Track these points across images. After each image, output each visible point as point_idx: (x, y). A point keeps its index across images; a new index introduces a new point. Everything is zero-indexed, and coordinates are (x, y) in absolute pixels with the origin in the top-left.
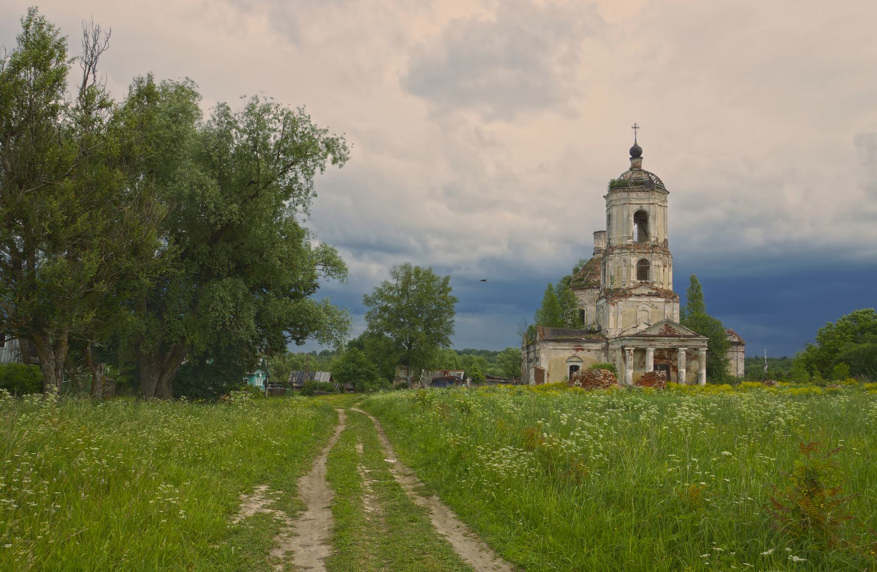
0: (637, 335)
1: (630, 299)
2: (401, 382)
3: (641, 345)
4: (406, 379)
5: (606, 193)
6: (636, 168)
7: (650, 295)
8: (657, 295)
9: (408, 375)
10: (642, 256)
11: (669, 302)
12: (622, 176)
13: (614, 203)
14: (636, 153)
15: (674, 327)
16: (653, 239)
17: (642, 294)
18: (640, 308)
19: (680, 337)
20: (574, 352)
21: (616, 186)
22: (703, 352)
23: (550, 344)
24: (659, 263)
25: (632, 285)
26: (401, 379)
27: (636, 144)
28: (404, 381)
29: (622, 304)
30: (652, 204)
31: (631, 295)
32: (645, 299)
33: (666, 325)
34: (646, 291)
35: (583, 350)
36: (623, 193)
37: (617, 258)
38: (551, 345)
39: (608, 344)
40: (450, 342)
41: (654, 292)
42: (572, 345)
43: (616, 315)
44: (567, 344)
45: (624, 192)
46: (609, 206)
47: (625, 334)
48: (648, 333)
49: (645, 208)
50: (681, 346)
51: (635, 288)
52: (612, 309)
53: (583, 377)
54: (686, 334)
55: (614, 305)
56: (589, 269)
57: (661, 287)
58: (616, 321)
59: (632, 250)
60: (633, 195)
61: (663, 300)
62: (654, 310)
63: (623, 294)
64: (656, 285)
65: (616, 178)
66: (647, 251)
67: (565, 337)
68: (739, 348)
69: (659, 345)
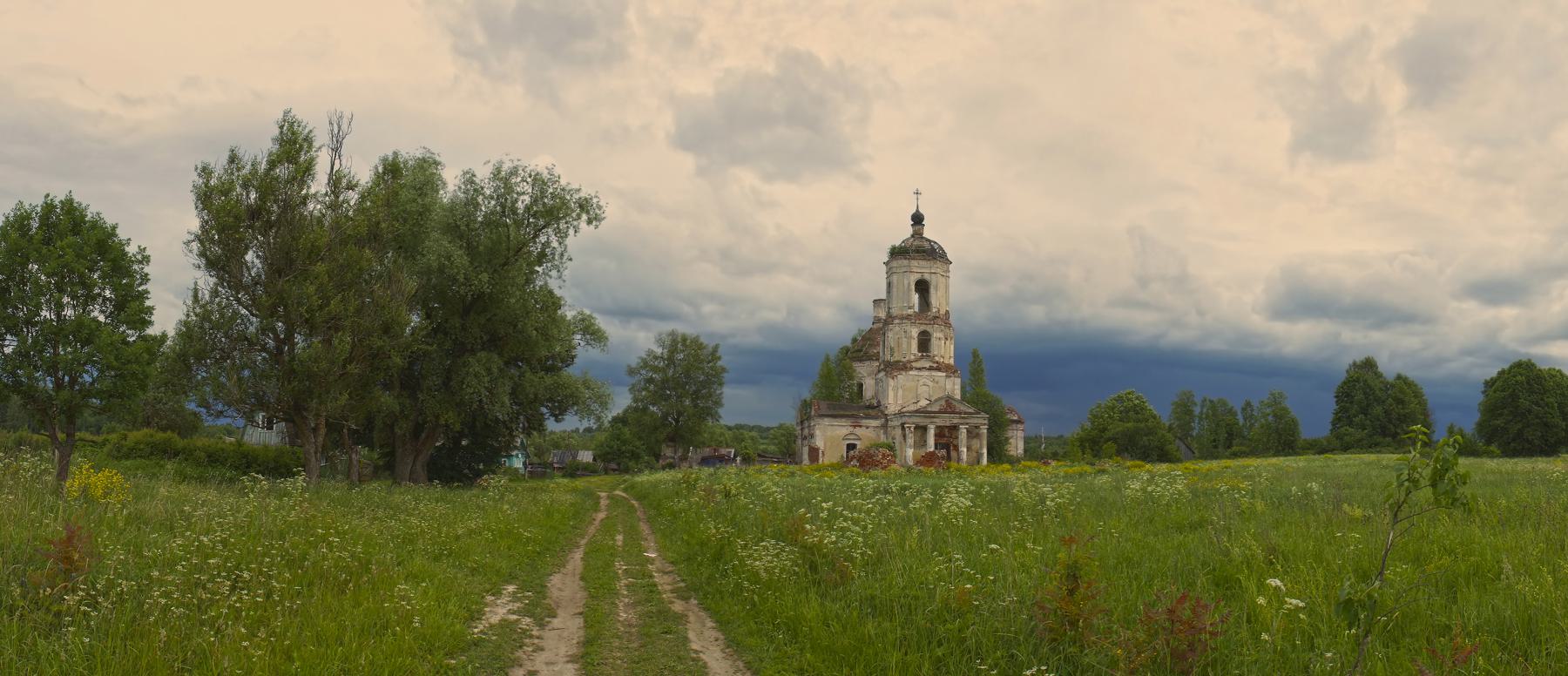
0: (917, 411)
1: (911, 373)
2: (668, 461)
3: (921, 421)
4: (673, 458)
5: (886, 259)
6: (918, 234)
7: (931, 369)
8: (938, 369)
9: (675, 453)
10: (923, 328)
11: (951, 377)
12: (903, 242)
13: (894, 270)
14: (918, 219)
15: (954, 403)
17: (923, 368)
18: (921, 383)
19: (960, 414)
20: (851, 429)
21: (897, 253)
22: (984, 431)
23: (826, 419)
24: (940, 335)
25: (913, 357)
26: (668, 458)
27: (917, 211)
28: (672, 460)
29: (902, 378)
30: (935, 273)
31: (911, 369)
32: (927, 373)
33: (947, 401)
34: (927, 366)
35: (860, 426)
36: (904, 261)
37: (897, 328)
38: (827, 421)
39: (887, 420)
40: (720, 417)
41: (935, 365)
42: (849, 421)
43: (896, 389)
44: (843, 420)
45: (906, 259)
46: (890, 273)
47: (904, 410)
48: (929, 409)
49: (927, 277)
50: (962, 424)
51: (916, 361)
52: (892, 382)
53: (860, 457)
54: (967, 411)
55: (893, 378)
56: (869, 339)
57: (942, 360)
58: (896, 396)
59: (913, 321)
60: (914, 263)
61: (944, 374)
62: (935, 385)
63: (904, 367)
64: (937, 359)
65: (897, 244)
66: (928, 322)
67: (842, 413)
68: (1019, 426)
69: (940, 422)
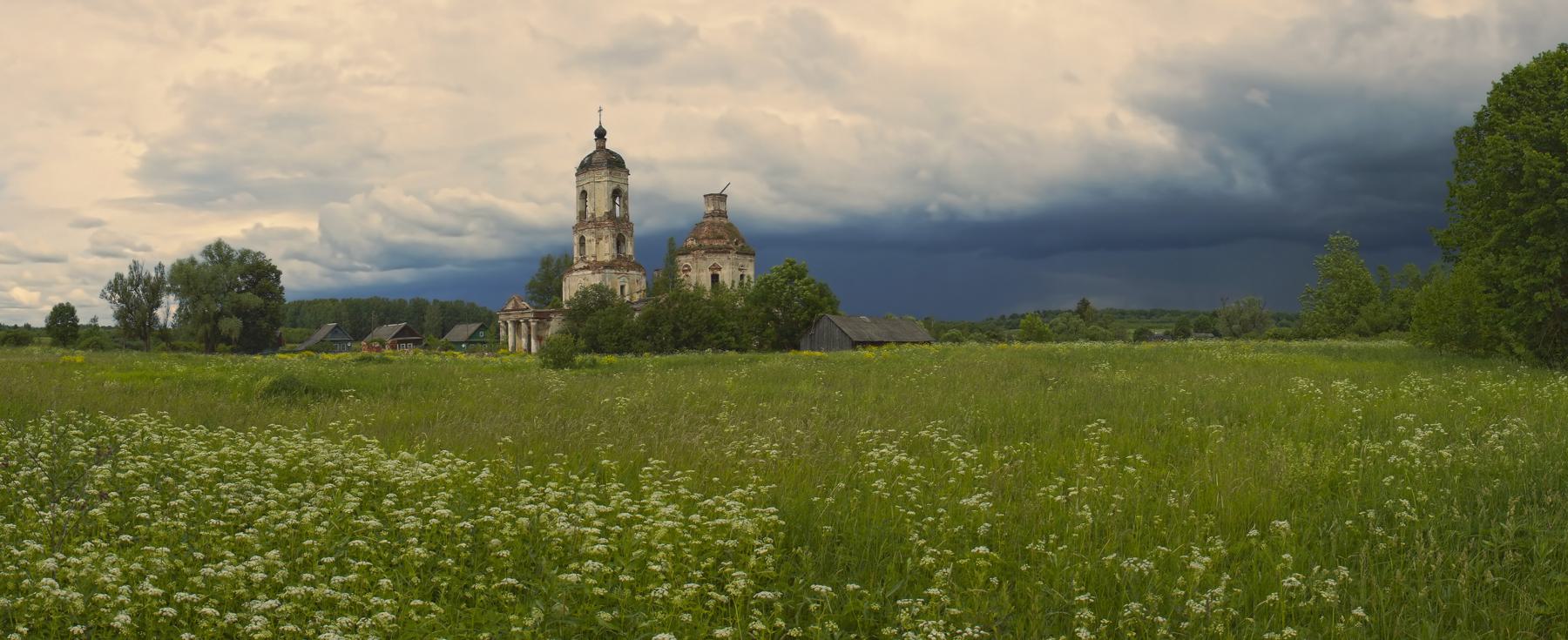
14: (601, 134)
16: (589, 216)
24: (592, 237)
27: (600, 126)
32: (581, 273)
34: (582, 267)
41: (586, 265)
57: (593, 259)
61: (590, 272)
